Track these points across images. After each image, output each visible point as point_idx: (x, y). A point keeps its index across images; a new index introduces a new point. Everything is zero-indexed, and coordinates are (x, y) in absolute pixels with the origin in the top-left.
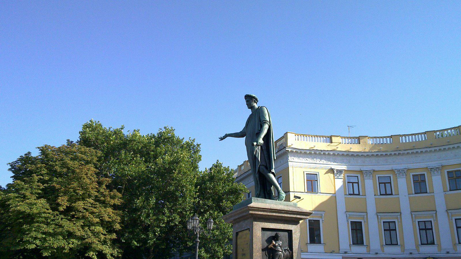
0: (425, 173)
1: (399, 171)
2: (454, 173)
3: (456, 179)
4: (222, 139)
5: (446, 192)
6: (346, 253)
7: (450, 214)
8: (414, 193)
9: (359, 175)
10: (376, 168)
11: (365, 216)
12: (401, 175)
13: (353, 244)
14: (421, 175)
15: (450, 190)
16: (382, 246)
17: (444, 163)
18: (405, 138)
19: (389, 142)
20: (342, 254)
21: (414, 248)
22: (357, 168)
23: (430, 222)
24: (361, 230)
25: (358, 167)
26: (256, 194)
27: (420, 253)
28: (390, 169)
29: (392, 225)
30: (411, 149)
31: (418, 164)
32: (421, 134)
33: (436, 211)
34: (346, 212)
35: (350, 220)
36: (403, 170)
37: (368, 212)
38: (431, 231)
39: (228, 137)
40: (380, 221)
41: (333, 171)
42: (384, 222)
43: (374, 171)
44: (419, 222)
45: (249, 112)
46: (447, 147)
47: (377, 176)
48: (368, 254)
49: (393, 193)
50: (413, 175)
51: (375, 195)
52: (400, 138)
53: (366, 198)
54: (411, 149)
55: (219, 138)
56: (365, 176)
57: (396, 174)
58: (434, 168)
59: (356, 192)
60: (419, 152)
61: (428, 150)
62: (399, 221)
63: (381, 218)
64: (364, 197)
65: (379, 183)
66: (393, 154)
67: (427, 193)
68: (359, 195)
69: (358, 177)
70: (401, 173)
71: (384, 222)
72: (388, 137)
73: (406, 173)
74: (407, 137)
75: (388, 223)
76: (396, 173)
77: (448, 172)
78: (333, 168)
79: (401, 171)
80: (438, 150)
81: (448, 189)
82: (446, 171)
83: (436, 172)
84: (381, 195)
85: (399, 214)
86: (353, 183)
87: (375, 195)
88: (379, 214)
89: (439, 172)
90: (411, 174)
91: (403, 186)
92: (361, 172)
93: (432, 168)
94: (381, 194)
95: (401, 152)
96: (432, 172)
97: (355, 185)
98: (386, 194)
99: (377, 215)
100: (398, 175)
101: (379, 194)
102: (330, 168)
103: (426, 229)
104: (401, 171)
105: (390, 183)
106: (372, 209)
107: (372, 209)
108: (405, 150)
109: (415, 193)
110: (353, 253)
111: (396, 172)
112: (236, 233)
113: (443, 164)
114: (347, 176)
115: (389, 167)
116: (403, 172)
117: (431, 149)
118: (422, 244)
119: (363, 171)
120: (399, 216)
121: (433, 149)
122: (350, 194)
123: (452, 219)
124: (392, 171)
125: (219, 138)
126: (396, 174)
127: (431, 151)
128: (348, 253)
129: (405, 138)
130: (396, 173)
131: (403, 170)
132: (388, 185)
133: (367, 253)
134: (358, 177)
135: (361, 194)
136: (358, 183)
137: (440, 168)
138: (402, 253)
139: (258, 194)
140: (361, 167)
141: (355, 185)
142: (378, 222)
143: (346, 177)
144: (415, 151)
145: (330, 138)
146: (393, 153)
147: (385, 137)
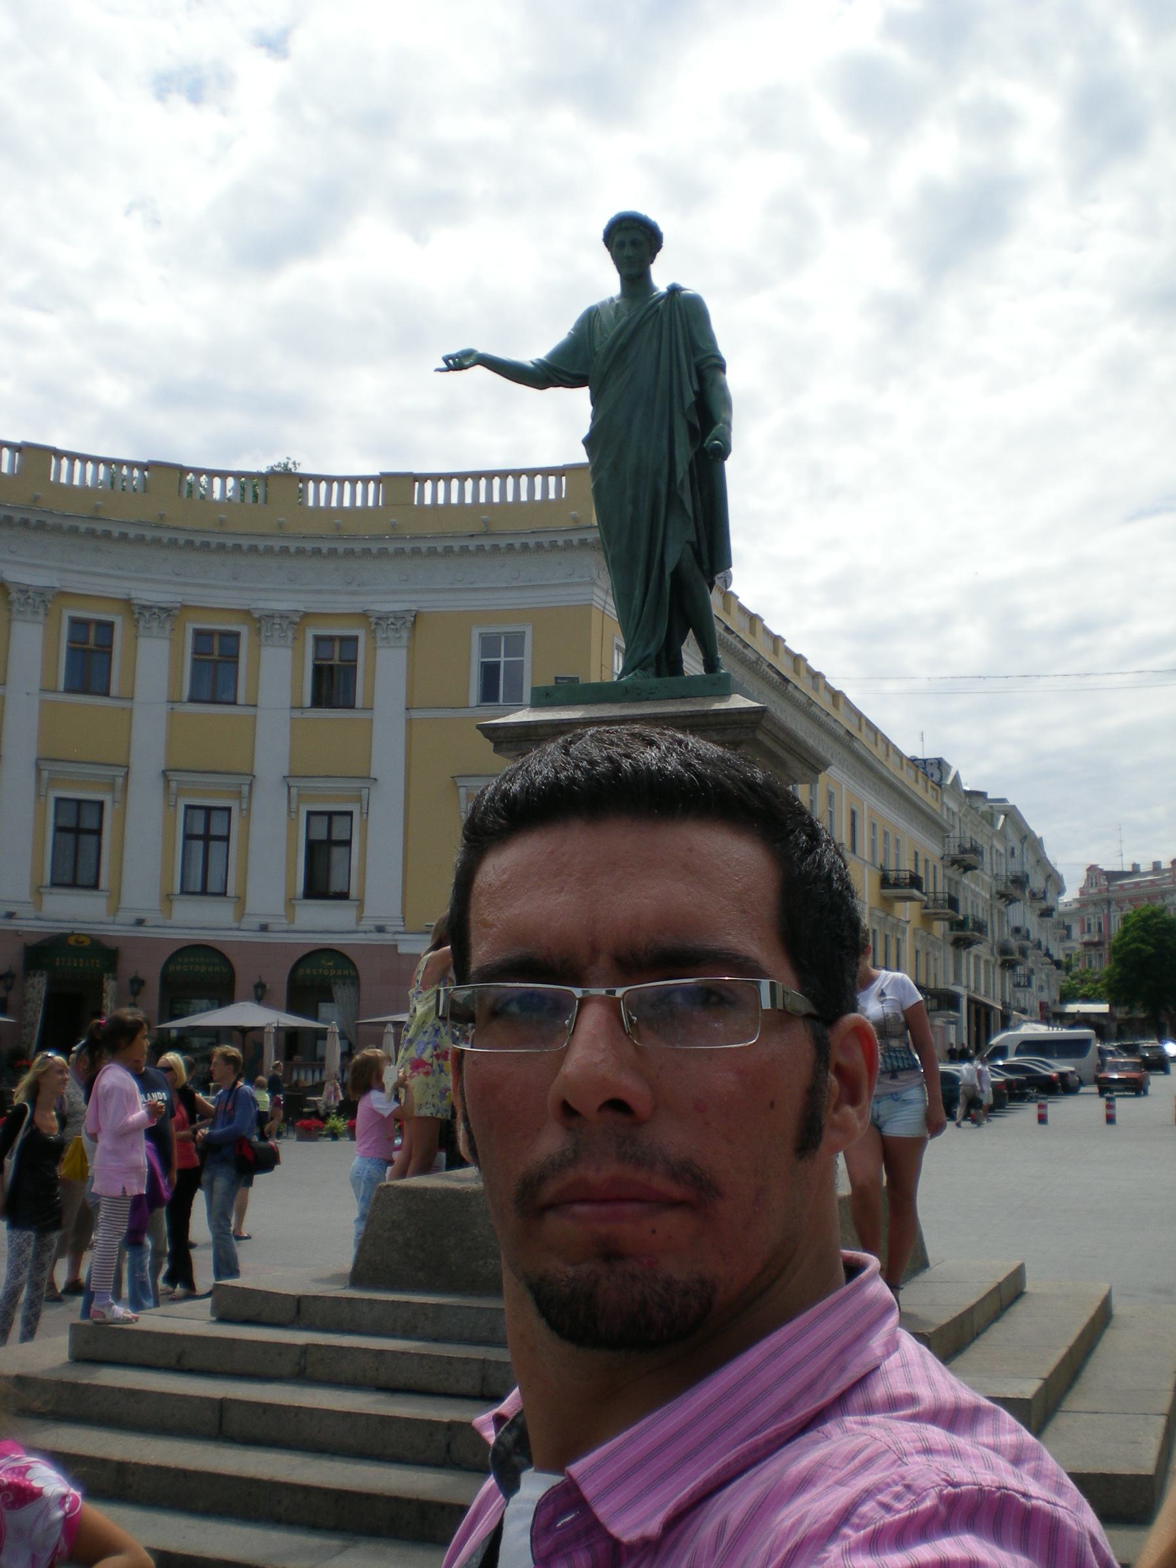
1: (24, 590)
2: (216, 640)
3: (219, 661)
5: (176, 706)
7: (173, 785)
8: (61, 686)
15: (193, 700)
17: (194, 597)
33: (128, 767)
36: (41, 592)
38: (94, 838)
39: (479, 371)
57: (10, 603)
58: (151, 607)
60: (116, 534)
70: (31, 601)
73: (49, 605)
74: (78, 464)
77: (198, 633)
80: (181, 542)
82: (190, 628)
83: (155, 624)
90: (67, 614)
93: (145, 607)
96: (142, 623)
100: (16, 606)
103: (78, 831)
111: (14, 595)
116: (38, 600)
117: (157, 533)
127: (157, 542)
129: (72, 465)
139: (648, 656)
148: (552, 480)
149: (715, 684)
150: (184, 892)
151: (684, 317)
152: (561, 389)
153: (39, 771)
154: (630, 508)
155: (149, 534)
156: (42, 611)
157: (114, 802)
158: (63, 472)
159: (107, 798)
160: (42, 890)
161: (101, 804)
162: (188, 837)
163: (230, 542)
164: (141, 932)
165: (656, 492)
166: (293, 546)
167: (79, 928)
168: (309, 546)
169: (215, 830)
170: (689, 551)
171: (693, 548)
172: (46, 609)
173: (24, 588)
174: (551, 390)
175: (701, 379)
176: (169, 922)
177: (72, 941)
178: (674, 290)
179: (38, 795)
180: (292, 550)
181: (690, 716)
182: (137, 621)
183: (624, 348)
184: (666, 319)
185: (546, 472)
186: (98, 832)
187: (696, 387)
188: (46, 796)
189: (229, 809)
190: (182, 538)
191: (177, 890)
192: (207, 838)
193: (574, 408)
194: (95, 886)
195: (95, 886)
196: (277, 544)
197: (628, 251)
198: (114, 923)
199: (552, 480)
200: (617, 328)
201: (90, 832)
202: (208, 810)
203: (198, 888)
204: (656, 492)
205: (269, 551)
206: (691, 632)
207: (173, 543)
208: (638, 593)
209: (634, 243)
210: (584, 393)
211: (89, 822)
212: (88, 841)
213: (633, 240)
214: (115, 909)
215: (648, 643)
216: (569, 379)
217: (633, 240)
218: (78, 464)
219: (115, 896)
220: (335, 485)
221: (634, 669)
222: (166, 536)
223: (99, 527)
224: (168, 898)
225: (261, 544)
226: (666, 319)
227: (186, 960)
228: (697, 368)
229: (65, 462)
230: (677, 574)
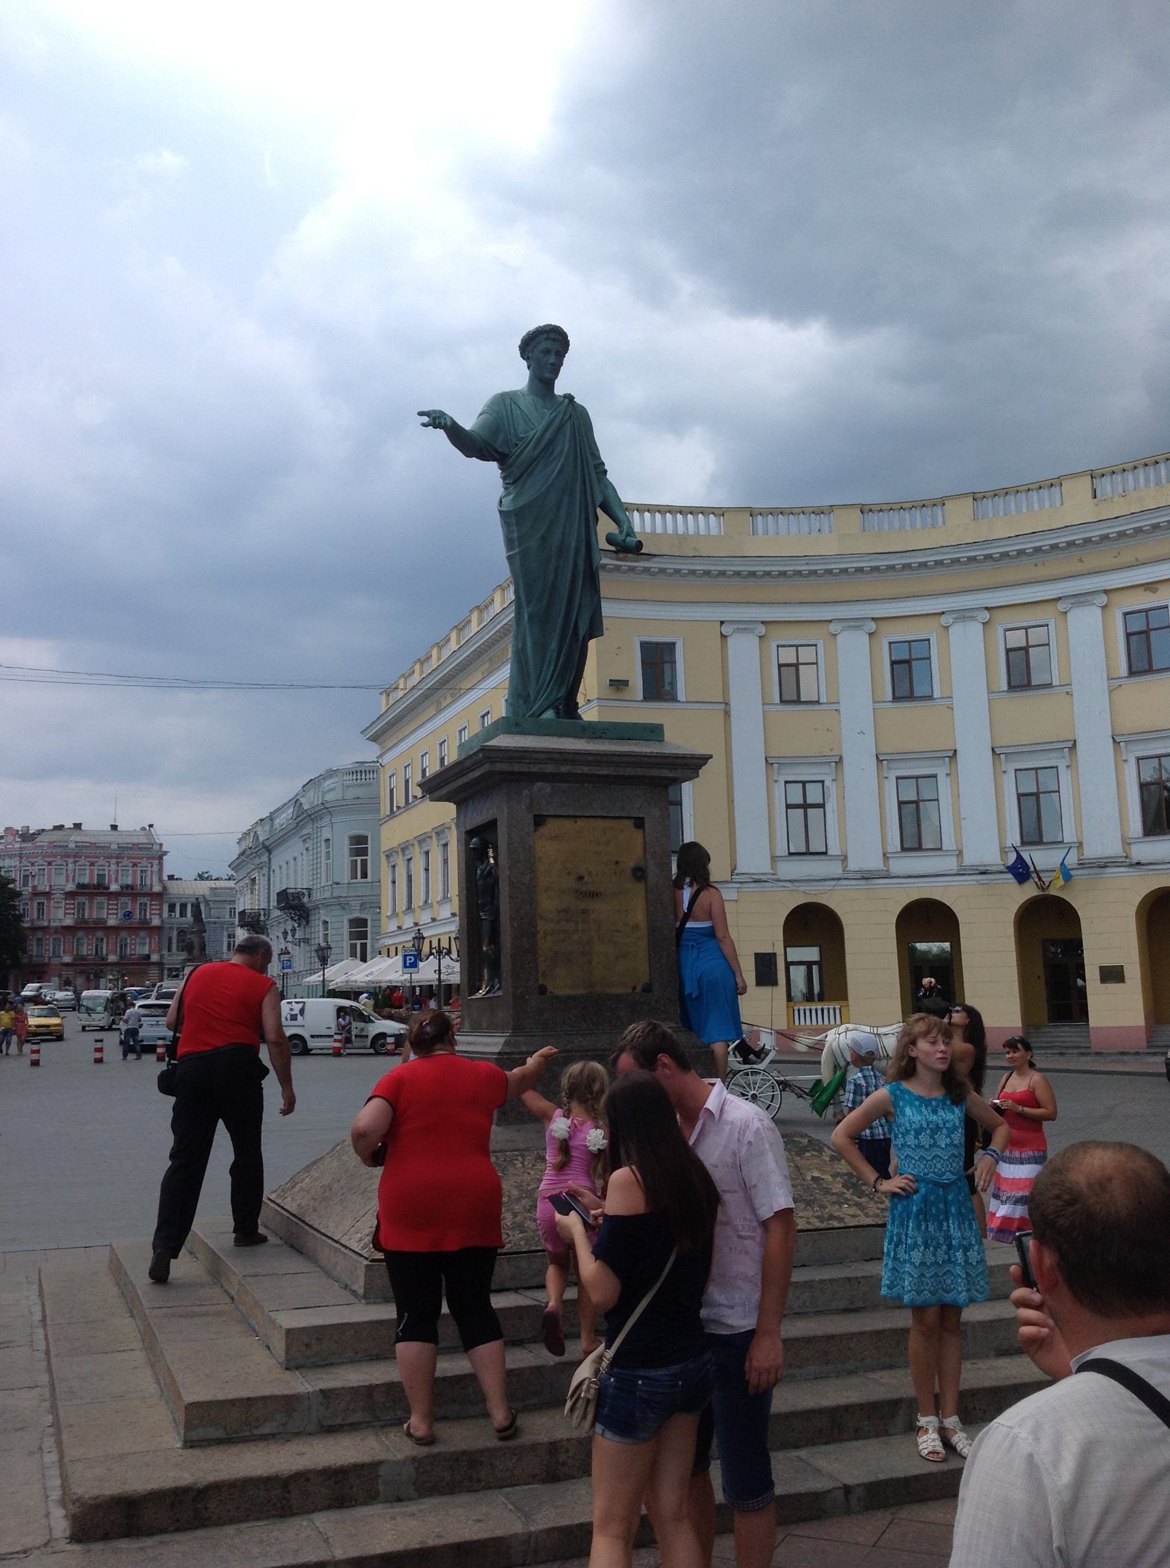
26: (552, 698)
112: (536, 816)
151: (573, 424)
154: (552, 576)
200: (544, 423)
208: (554, 645)
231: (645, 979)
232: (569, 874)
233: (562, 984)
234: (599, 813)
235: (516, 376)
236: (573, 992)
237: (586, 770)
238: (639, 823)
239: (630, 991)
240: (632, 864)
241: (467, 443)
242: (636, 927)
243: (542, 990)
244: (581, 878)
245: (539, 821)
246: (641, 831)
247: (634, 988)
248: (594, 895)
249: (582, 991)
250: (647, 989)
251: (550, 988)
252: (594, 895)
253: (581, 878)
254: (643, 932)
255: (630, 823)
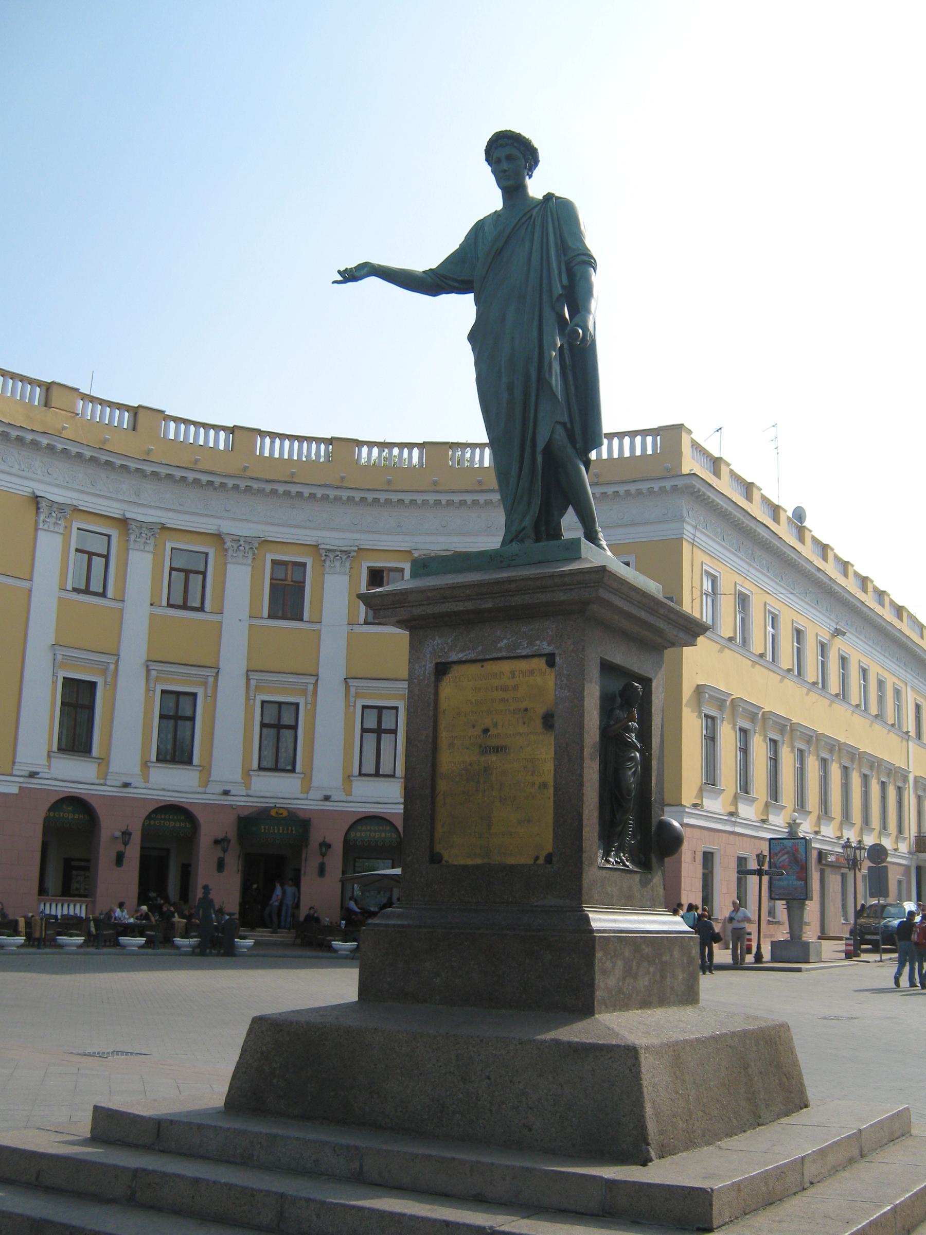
0: (309, 562)
4: (350, 276)
6: (33, 775)
7: (353, 690)
8: (266, 614)
9: (115, 534)
10: (172, 519)
11: (112, 667)
12: (241, 554)
13: (60, 749)
14: (295, 564)
15: (366, 623)
16: (145, 765)
17: (366, 540)
18: (273, 442)
19: (221, 447)
20: (21, 780)
21: (238, 777)
22: (114, 509)
23: (294, 707)
24: (91, 708)
25: (116, 505)
27: (250, 793)
28: (212, 529)
29: (185, 703)
30: (286, 482)
31: (293, 529)
32: (319, 440)
33: (317, 675)
34: (56, 647)
35: (62, 674)
36: (249, 541)
37: (123, 654)
38: (291, 732)
39: (374, 281)
40: (152, 685)
41: (38, 503)
42: (163, 692)
43: (164, 528)
44: (263, 702)
45: (489, 199)
46: (382, 497)
47: (169, 546)
48: (101, 785)
49: (208, 607)
50: (274, 562)
51: (151, 605)
52: (259, 439)
53: (122, 610)
54: (286, 482)
55: (339, 272)
56: (132, 537)
57: (226, 550)
59: (96, 586)
61: (332, 493)
62: (210, 692)
63: (158, 679)
64: (119, 605)
65: (172, 569)
66: (230, 486)
67: (301, 620)
68: (103, 595)
69: (109, 536)
71: (163, 692)
72: (223, 428)
74: (278, 441)
75: (174, 697)
76: (226, 547)
78: (38, 493)
79: (242, 543)
81: (362, 620)
83: (337, 564)
84: (170, 605)
85: (212, 672)
86: (91, 554)
87: (151, 605)
88: (153, 666)
89: (348, 564)
90: (269, 557)
91: (240, 588)
92: (123, 523)
93: (329, 550)
94: (172, 602)
95: (256, 486)
96: (328, 563)
97: (98, 563)
98: (185, 607)
99: (147, 667)
100: (230, 553)
101: (165, 603)
102: (30, 490)
103: (278, 727)
104: (242, 543)
105: (204, 574)
106: (134, 647)
107: (134, 647)
108: (268, 481)
109: (270, 617)
110: (56, 779)
111: (228, 544)
113: (362, 542)
114: (79, 529)
115: (208, 525)
116: (248, 547)
118: (261, 769)
119: (131, 522)
120: (211, 679)
121: (345, 494)
122: (75, 590)
123: (354, 706)
124: (218, 538)
125: (339, 272)
126: (226, 550)
127: (337, 499)
128: (41, 775)
129: (273, 442)
130: (226, 547)
131: (249, 540)
132: (196, 580)
133: (97, 781)
134: (109, 536)
135: (110, 593)
136: (107, 557)
137: (353, 554)
138: (201, 790)
139: (524, 528)
140: (124, 506)
141: (98, 563)
142: (148, 690)
143: (74, 532)
144: (294, 489)
145: (44, 388)
146: (230, 483)
147: (214, 427)
148: (649, 439)
149: (567, 549)
150: (360, 774)
152: (453, 296)
153: (248, 680)
155: (332, 493)
156: (250, 555)
157: (306, 703)
158: (266, 447)
159: (301, 701)
160: (150, 764)
161: (297, 705)
162: (364, 731)
163: (395, 497)
164: (328, 806)
165: (527, 378)
166: (444, 498)
167: (281, 803)
168: (456, 498)
169: (387, 724)
170: (560, 430)
171: (566, 429)
172: (254, 554)
173: (237, 538)
174: (444, 297)
175: (571, 275)
176: (350, 798)
177: (273, 813)
178: (549, 197)
179: (248, 699)
180: (444, 502)
181: (538, 578)
182: (324, 561)
183: (499, 252)
184: (538, 223)
185: (644, 433)
186: (295, 728)
187: (565, 281)
188: (254, 699)
189: (396, 708)
190: (357, 495)
191: (356, 772)
192: (379, 731)
193: (461, 309)
194: (293, 770)
195: (293, 770)
196: (432, 498)
197: (505, 165)
198: (307, 799)
199: (649, 439)
201: (83, 707)
202: (380, 709)
203: (373, 771)
204: (527, 378)
205: (425, 503)
206: (570, 510)
207: (350, 499)
208: (514, 472)
209: (509, 158)
210: (470, 297)
211: (287, 719)
212: (286, 734)
213: (511, 155)
214: (206, 781)
215: (524, 517)
216: (456, 285)
217: (511, 155)
218: (278, 441)
219: (206, 770)
220: (478, 451)
221: (512, 541)
222: (345, 494)
223: (294, 489)
224: (348, 778)
225: (419, 498)
226: (538, 223)
227: (364, 828)
228: (567, 264)
229: (268, 440)
230: (548, 451)
231: (549, 848)
232: (474, 727)
233: (458, 852)
234: (504, 654)
235: (489, 199)
236: (469, 862)
237: (469, 605)
238: (551, 660)
239: (531, 862)
240: (541, 710)
241: (432, 283)
242: (544, 785)
243: (436, 859)
244: (486, 731)
245: (442, 670)
246: (553, 669)
247: (537, 858)
248: (498, 750)
249: (479, 861)
250: (549, 859)
251: (445, 858)
252: (498, 750)
253: (486, 731)
254: (551, 790)
255: (540, 663)
